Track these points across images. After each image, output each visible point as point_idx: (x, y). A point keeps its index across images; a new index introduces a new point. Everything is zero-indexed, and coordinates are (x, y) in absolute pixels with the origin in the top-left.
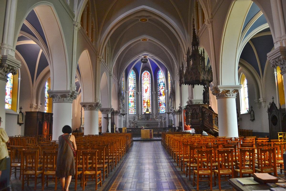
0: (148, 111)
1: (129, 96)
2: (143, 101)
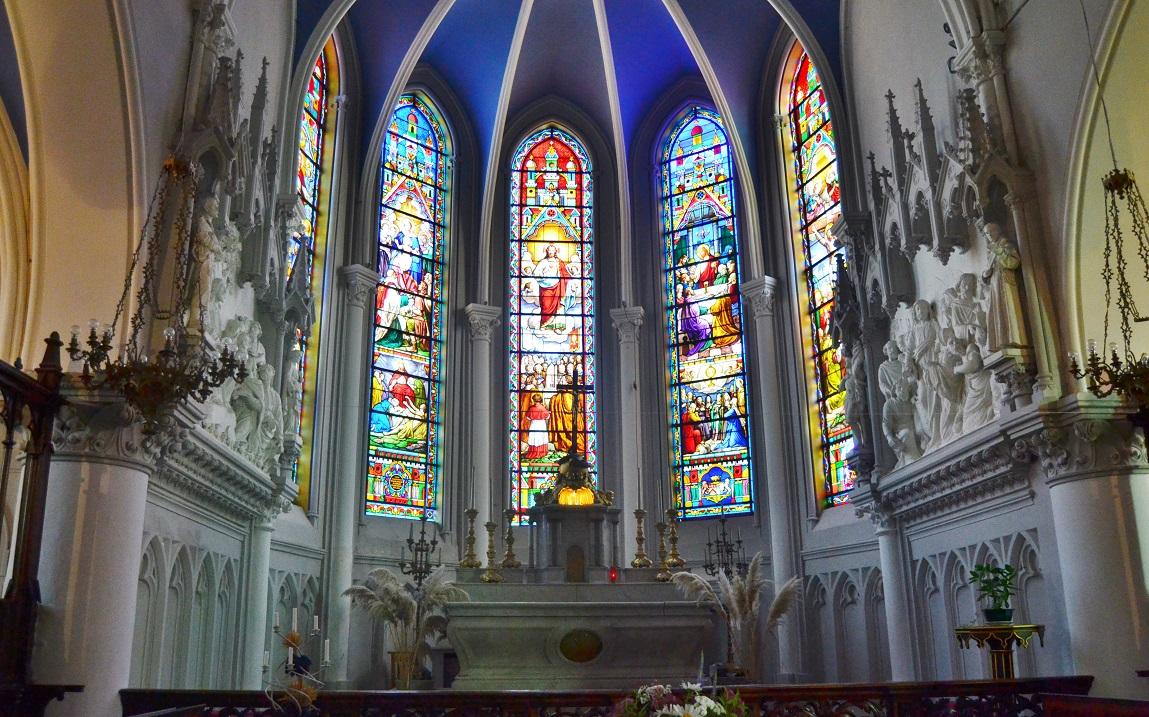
1: (380, 333)
2: (514, 397)
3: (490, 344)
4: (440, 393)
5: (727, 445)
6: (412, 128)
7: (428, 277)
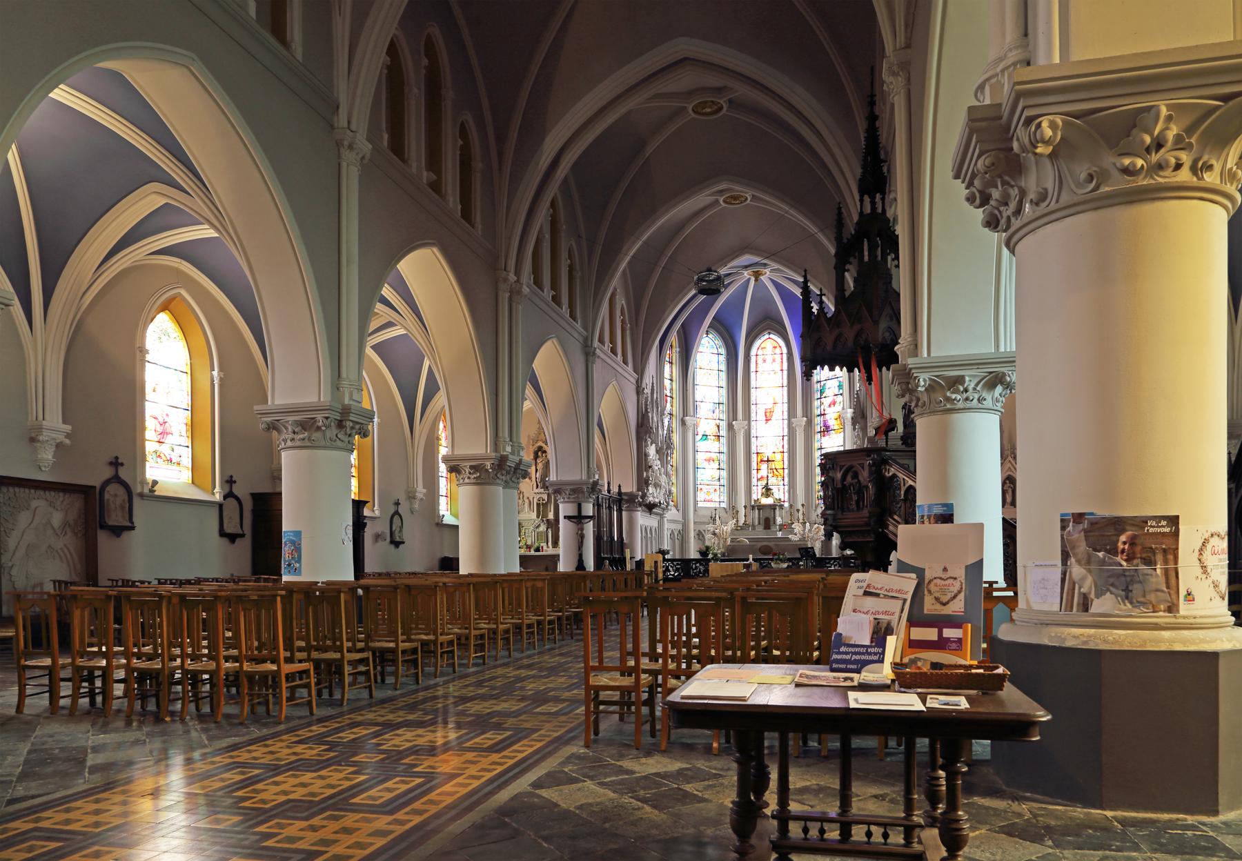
1: (698, 438)
2: (754, 457)
4: (724, 457)
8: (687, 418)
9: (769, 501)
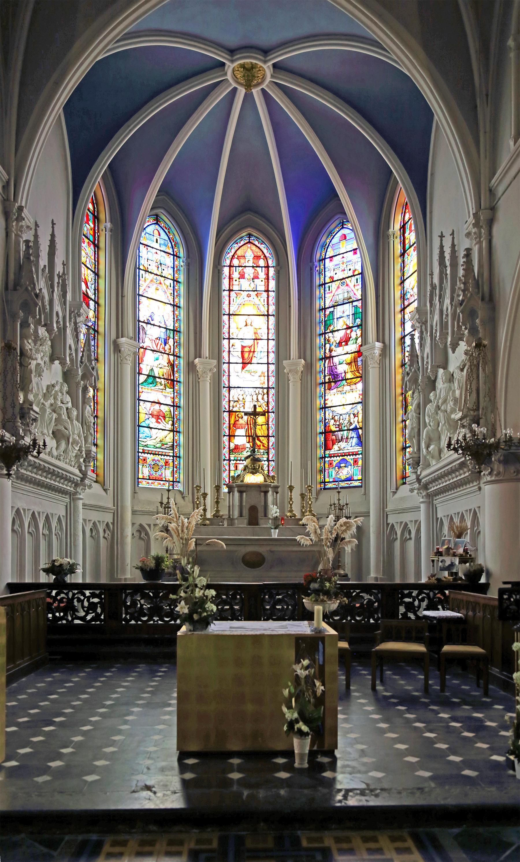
0: (254, 471)
3: (210, 383)
4: (181, 414)
5: (350, 445)
6: (157, 239)
7: (171, 342)
8: (123, 340)
9: (258, 479)
